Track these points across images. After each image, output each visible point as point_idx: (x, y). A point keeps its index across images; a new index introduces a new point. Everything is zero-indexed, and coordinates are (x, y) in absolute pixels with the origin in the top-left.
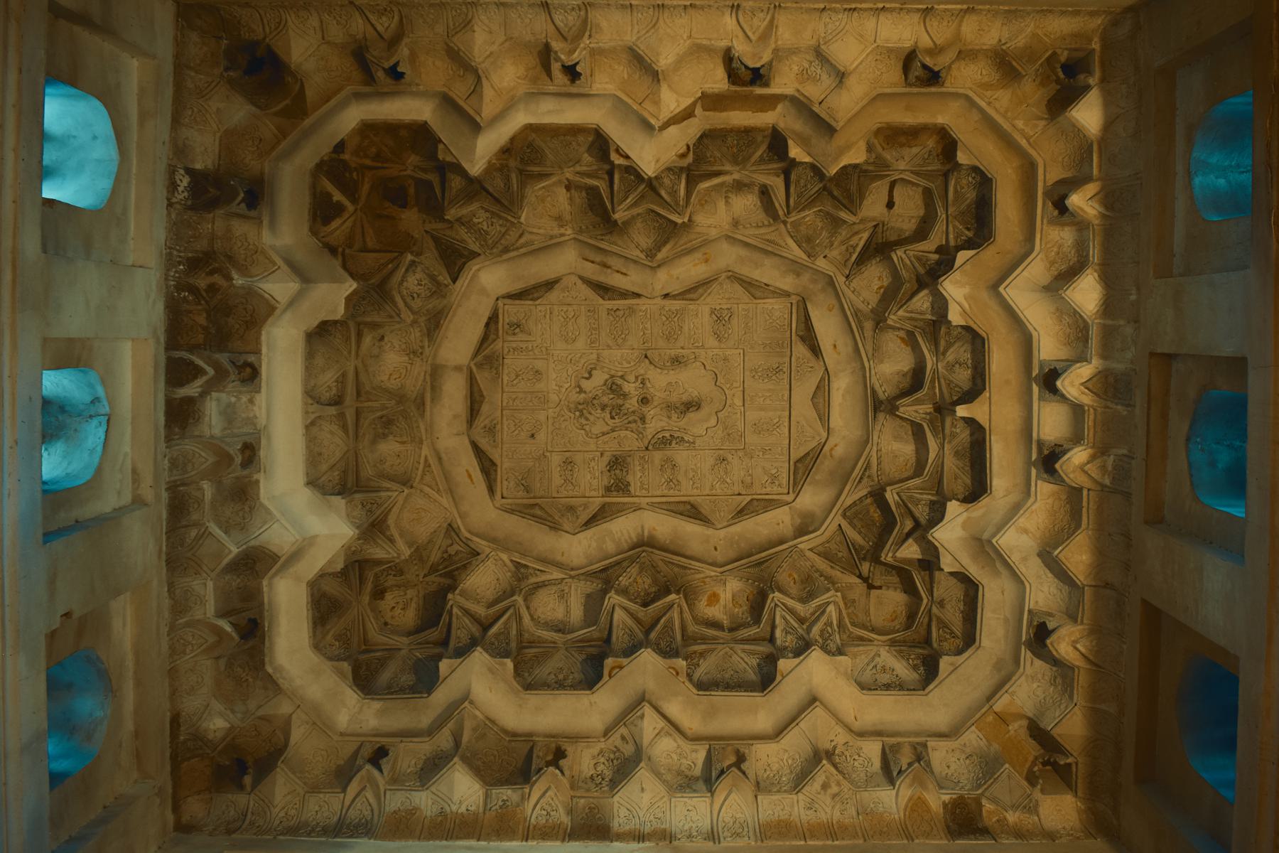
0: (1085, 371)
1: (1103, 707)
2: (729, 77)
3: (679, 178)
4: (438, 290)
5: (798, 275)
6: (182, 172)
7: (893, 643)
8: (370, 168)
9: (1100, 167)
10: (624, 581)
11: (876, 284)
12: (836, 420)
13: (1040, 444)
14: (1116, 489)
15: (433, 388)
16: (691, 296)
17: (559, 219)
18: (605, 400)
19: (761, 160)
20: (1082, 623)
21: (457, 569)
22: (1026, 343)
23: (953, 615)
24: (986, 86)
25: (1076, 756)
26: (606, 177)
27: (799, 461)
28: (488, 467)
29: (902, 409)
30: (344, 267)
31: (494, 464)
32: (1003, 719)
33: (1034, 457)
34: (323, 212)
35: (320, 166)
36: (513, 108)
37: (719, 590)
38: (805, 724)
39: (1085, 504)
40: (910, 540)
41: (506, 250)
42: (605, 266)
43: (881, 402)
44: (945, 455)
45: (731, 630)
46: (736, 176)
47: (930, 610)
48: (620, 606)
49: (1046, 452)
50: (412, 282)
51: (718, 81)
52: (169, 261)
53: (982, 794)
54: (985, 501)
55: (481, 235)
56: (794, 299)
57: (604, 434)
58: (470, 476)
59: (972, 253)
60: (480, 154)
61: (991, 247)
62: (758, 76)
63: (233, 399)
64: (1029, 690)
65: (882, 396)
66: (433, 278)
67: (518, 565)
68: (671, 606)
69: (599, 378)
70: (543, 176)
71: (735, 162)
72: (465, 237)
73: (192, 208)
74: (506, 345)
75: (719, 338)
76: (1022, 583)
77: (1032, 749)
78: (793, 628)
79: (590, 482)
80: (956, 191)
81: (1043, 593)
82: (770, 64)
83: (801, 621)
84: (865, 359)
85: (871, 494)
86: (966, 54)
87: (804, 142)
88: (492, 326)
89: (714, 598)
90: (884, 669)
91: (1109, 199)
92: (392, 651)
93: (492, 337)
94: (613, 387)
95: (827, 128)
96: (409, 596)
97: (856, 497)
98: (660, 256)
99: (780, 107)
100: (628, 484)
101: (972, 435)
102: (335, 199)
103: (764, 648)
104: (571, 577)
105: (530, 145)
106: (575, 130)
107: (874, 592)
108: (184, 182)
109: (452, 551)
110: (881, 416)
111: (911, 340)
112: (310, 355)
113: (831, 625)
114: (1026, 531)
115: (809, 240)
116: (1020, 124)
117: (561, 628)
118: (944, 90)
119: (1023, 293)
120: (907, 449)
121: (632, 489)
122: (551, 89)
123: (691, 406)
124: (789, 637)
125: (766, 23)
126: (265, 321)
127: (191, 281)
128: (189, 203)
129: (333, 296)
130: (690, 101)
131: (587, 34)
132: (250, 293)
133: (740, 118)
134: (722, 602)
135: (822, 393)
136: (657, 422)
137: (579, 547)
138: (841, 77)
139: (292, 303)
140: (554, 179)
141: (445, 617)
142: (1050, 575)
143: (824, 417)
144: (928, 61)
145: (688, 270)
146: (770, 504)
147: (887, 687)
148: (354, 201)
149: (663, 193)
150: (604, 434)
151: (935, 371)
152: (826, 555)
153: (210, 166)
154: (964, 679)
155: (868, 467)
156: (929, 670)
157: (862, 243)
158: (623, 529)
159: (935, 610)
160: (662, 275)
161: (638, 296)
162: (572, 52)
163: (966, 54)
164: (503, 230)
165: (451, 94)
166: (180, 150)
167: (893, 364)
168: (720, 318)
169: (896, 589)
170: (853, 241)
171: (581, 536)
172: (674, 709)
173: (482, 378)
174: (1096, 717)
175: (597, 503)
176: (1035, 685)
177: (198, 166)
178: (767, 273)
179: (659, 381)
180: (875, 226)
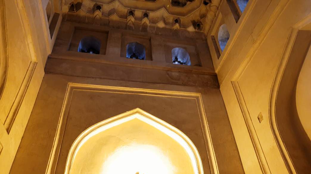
1: (86, 19)
9: (182, 29)
13: (134, 11)
14: (127, 27)
22: (152, 10)
24: (200, 11)
25: (75, 13)
33: (132, 9)
39: (124, 19)
49: (133, 12)
59: (171, 2)
61: (171, 6)
76: (108, 4)
81: (106, 8)
86: (207, 11)
91: (176, 31)
114: (118, 6)
116: (192, 15)
118: (202, 3)
163: (207, 11)
176: (88, 4)
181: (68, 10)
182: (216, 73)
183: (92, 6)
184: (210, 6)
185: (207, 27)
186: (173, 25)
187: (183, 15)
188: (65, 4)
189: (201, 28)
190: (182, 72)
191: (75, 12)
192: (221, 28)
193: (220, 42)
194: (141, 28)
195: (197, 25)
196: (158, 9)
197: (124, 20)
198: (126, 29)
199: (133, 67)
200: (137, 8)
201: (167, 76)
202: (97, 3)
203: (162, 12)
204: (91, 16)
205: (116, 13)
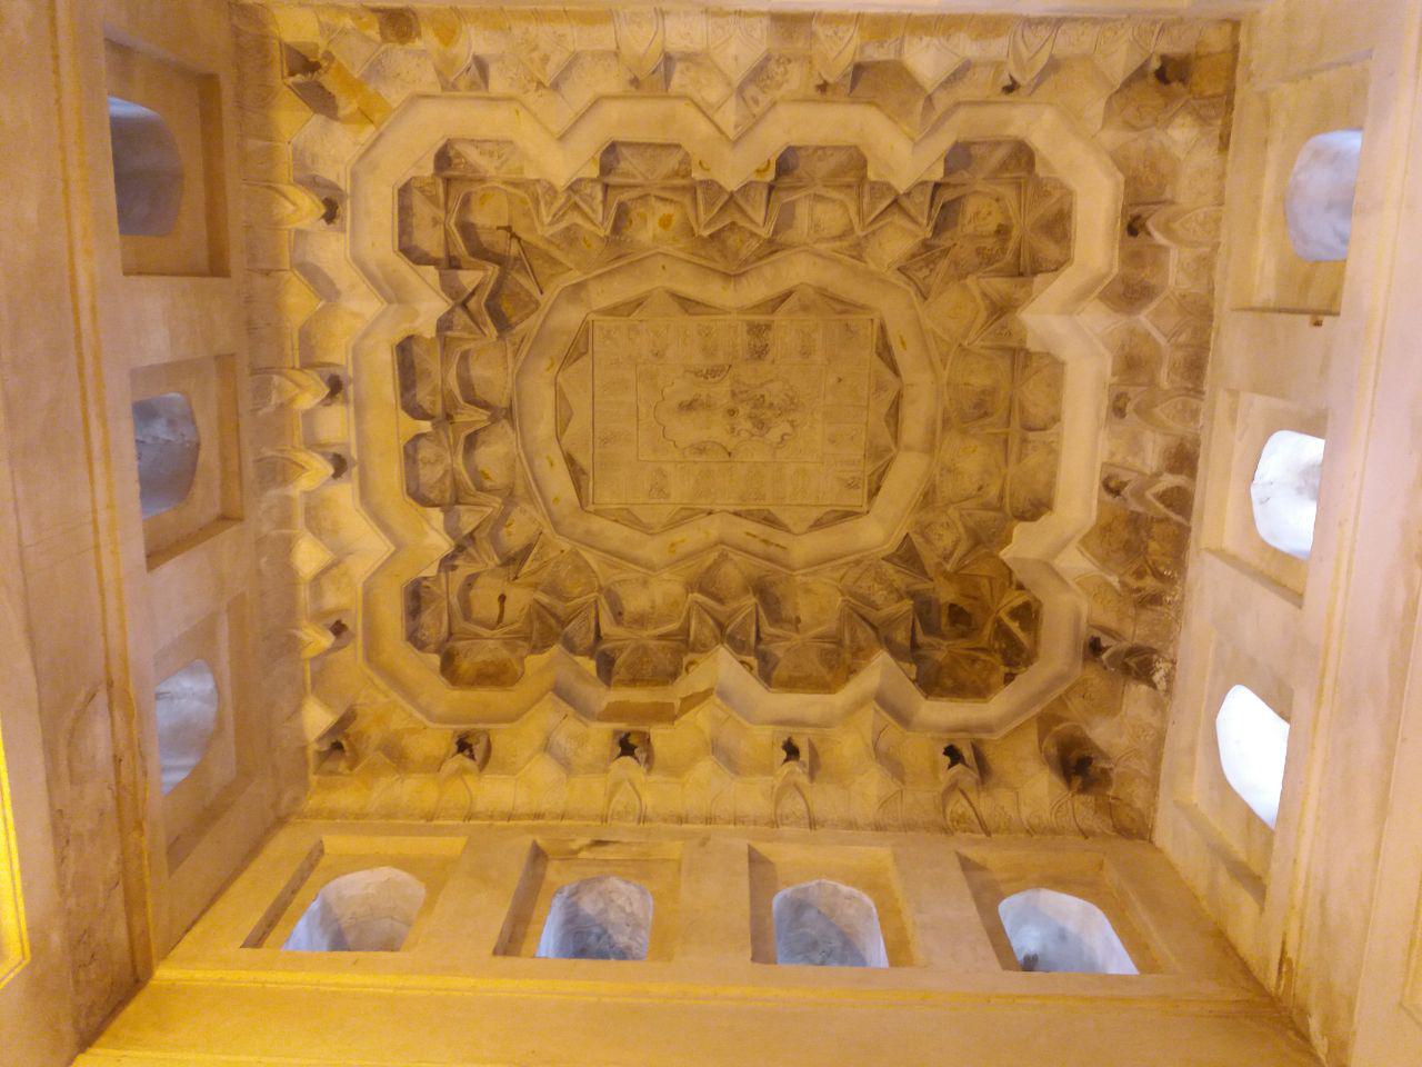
0: (305, 483)
1: (260, 143)
2: (649, 740)
3: (696, 637)
4: (924, 530)
5: (588, 532)
6: (1159, 687)
7: (482, 180)
8: (982, 650)
10: (755, 244)
11: (513, 529)
12: (549, 394)
13: (346, 401)
15: (933, 433)
16: (684, 513)
17: (808, 591)
18: (769, 414)
19: (621, 650)
20: (290, 231)
21: (921, 255)
23: (423, 210)
26: (762, 635)
27: (585, 353)
28: (885, 352)
29: (485, 418)
30: (1010, 572)
31: (879, 355)
32: (365, 116)
34: (1028, 614)
35: (1029, 662)
36: (845, 714)
37: (659, 230)
38: (569, 116)
40: (470, 290)
41: (858, 563)
42: (766, 542)
43: (505, 417)
44: (439, 377)
45: (647, 195)
46: (645, 634)
47: (447, 212)
48: (758, 226)
50: (947, 538)
51: (660, 735)
52: (1179, 608)
53: (380, 46)
54: (398, 338)
55: (880, 578)
56: (591, 508)
57: (772, 381)
58: (903, 343)
60: (879, 671)
62: (626, 748)
63: (1130, 459)
64: (335, 147)
65: (504, 422)
66: (928, 541)
67: (859, 258)
68: (708, 225)
69: (774, 435)
70: (821, 638)
71: (645, 649)
72: (896, 577)
73: (1153, 651)
74: (861, 469)
75: (661, 472)
77: (329, 81)
78: (584, 201)
79: (786, 331)
80: (441, 623)
81: (331, 250)
82: (612, 761)
83: (576, 207)
84: (522, 455)
85: (511, 327)
87: (581, 675)
88: (874, 486)
89: (665, 222)
90: (491, 154)
92: (994, 176)
93: (875, 477)
94: (761, 425)
95: (562, 692)
96: (973, 225)
97: (525, 324)
98: (714, 556)
99: (604, 704)
100: (748, 332)
101: (415, 395)
102: (1017, 624)
103: (612, 180)
104: (805, 244)
105: (831, 668)
106: (791, 685)
107: (504, 223)
108: (1157, 677)
109: (926, 272)
110: (505, 404)
111: (479, 477)
112: (1051, 485)
113: (549, 204)
114: (355, 315)
115: (577, 569)
117: (819, 198)
118: (454, 727)
119: (369, 546)
120: (478, 371)
121: (746, 328)
122: (808, 731)
123: (688, 407)
124: (588, 191)
125: (615, 800)
126: (1093, 529)
127: (1160, 585)
128: (1155, 657)
129: (1024, 546)
130: (684, 718)
131: (775, 789)
132: (1103, 561)
133: (639, 696)
134: (657, 218)
135: (563, 421)
136: (721, 391)
137: (797, 271)
138: (547, 747)
139: (1065, 544)
140: (812, 633)
141: (935, 213)
142: (326, 270)
143: (560, 396)
144: (468, 763)
145: (690, 537)
146: (612, 311)
147: (485, 141)
148: (999, 622)
149: (711, 622)
150: (772, 381)
151: (454, 454)
152: (553, 261)
153: (1133, 688)
154: (407, 152)
155: (516, 353)
156: (444, 159)
157: (528, 563)
158: (756, 289)
159: (441, 214)
160: (714, 533)
161: (737, 514)
162: (791, 773)
163: (434, 766)
164: (859, 583)
165: (901, 729)
166: (1159, 707)
167: (494, 455)
168: (660, 490)
169: (483, 227)
170: (536, 565)
171: (796, 282)
172: (704, 127)
173: (885, 438)
174: (266, 132)
175: (779, 318)
177: (1144, 688)
178: (616, 534)
179: (717, 431)
180: (516, 578)
181: (288, 38)
182: (149, 973)
183: (331, 177)
184: (461, 772)
185: (346, 797)
186: (319, 616)
187: (371, 653)
188: (326, 29)
189: (328, 765)
190: (118, 772)
191: (283, 77)
192: (385, 873)
193: (315, 906)
194: (270, 453)
195: (339, 744)
196: (385, 527)
197: (293, 357)
198: (255, 371)
199: (90, 460)
200: (360, 410)
201: (81, 697)
202: (348, 202)
203: (369, 546)
204: (284, 171)
205: (324, 307)
